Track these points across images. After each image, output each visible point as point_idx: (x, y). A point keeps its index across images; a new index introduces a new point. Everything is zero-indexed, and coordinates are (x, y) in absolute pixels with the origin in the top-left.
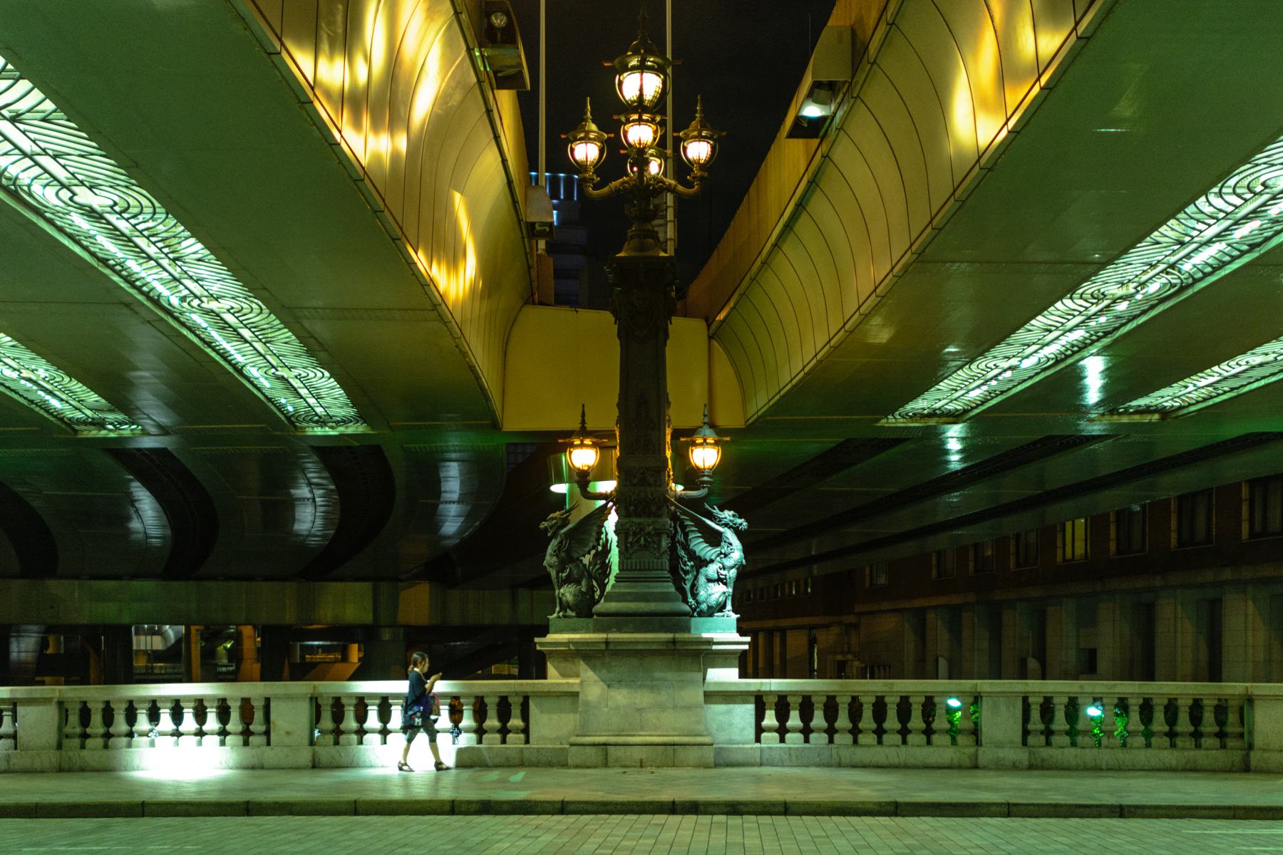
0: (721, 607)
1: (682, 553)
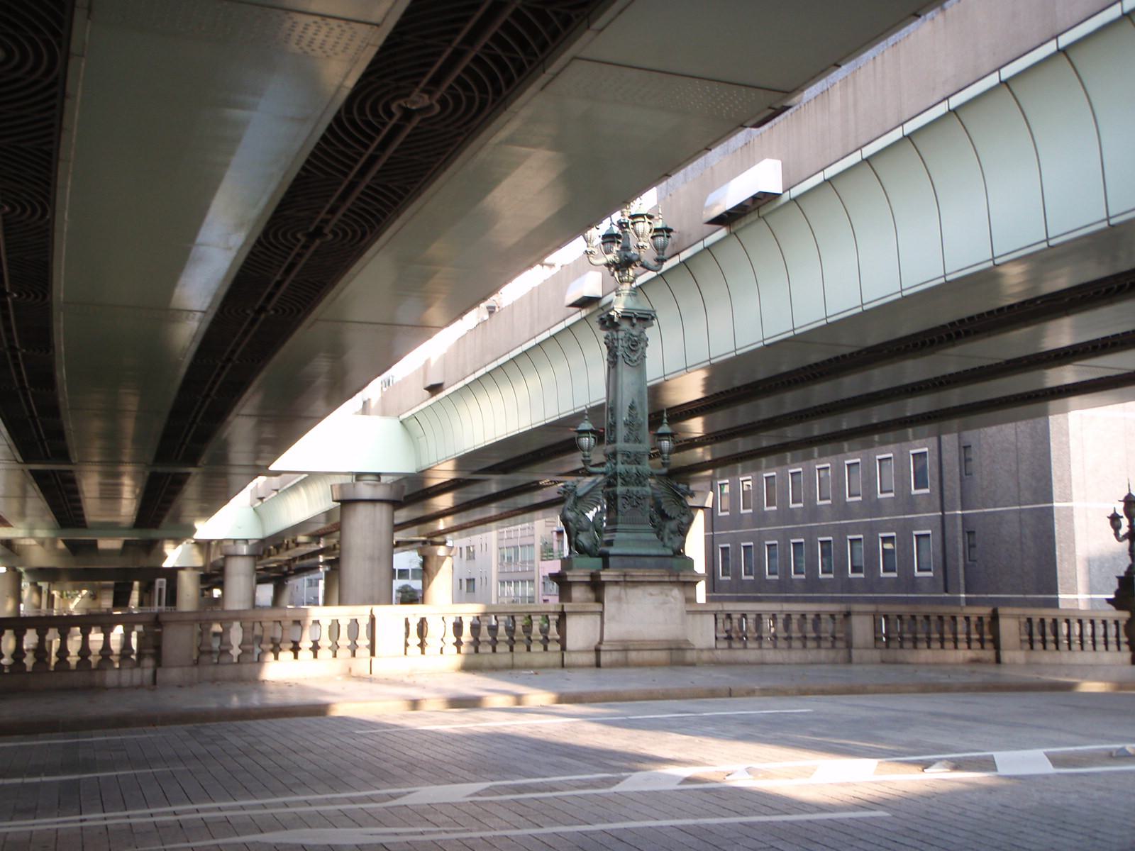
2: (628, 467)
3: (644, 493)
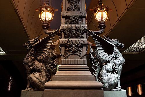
0: (115, 86)
1: (93, 58)
2: (69, 26)
3: (81, 42)
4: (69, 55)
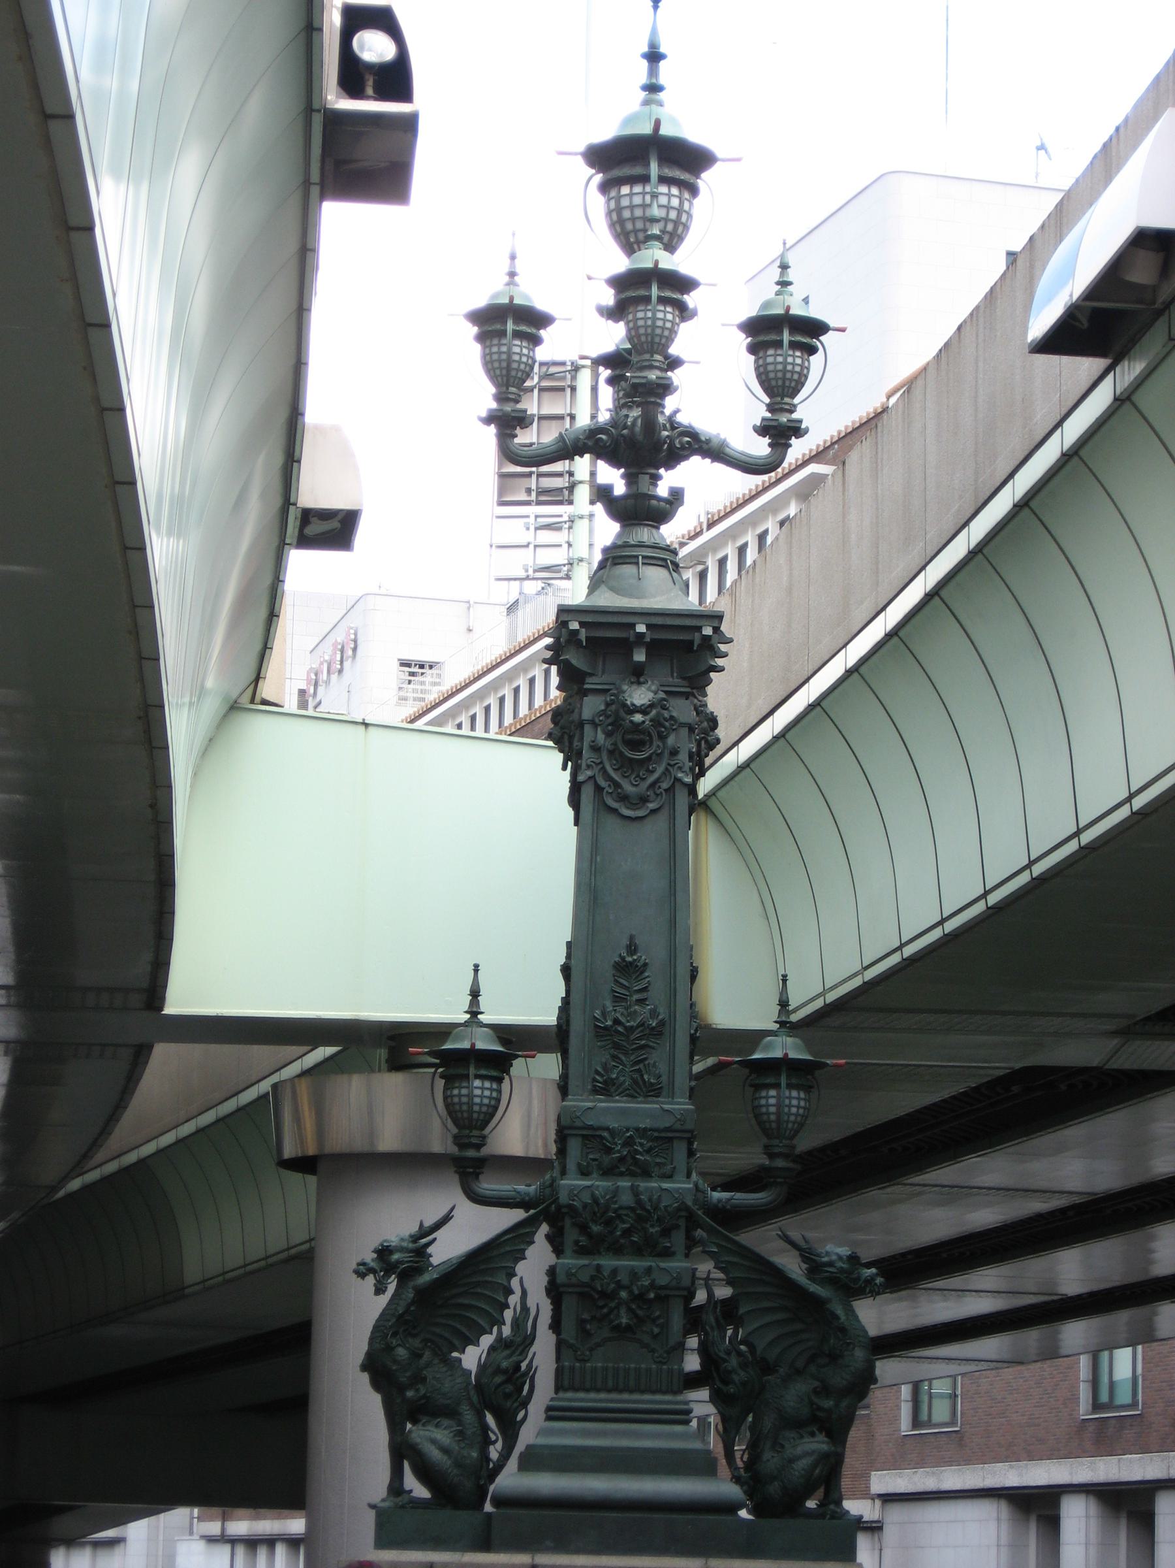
2: (601, 1185)
3: (663, 1280)
4: (598, 1345)
